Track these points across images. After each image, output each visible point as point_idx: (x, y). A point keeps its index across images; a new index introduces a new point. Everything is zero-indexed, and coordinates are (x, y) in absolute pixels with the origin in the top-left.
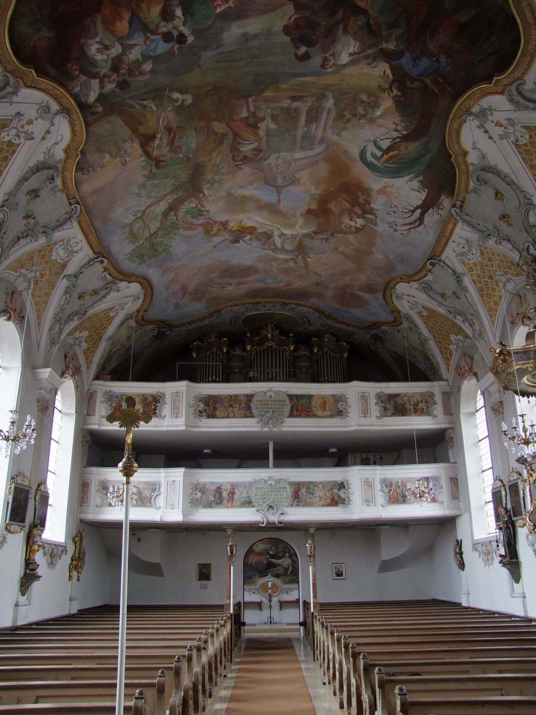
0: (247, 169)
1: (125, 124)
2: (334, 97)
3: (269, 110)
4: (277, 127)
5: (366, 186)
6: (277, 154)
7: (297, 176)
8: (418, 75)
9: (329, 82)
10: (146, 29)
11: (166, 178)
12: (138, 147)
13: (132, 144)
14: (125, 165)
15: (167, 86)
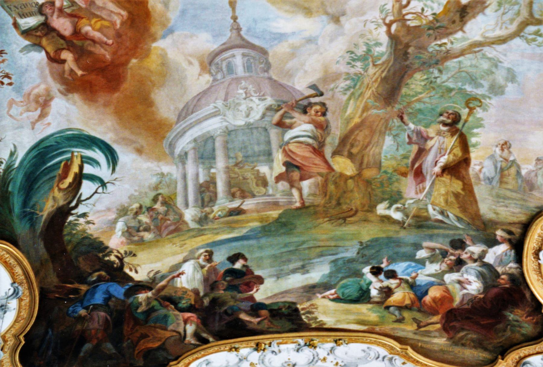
0: (301, 85)
1: (476, 202)
2: (186, 223)
3: (271, 191)
4: (257, 168)
5: (76, 97)
6: (252, 121)
7: (207, 78)
8: (97, 286)
9: (199, 239)
10: (412, 286)
11: (450, 90)
12: (473, 162)
13: (480, 171)
14: (506, 143)
15: (405, 228)
